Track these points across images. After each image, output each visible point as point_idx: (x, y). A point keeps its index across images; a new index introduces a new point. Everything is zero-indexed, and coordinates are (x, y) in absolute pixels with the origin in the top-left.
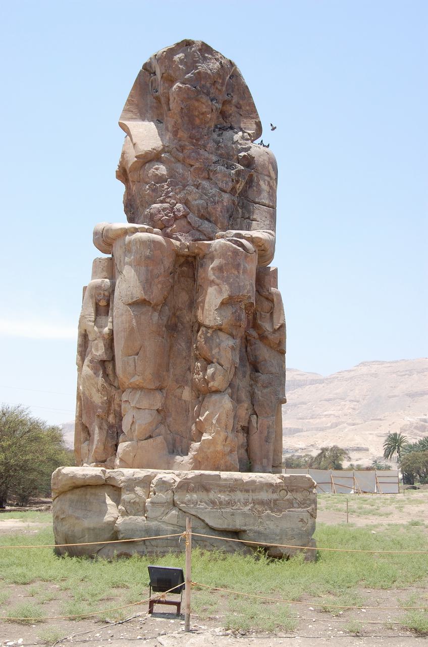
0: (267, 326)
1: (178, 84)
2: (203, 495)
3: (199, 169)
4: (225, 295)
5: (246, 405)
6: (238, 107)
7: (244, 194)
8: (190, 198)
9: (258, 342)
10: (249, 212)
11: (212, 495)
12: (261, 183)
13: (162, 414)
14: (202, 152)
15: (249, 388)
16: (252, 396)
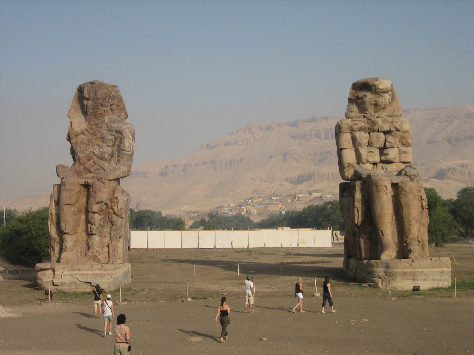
0: (116, 209)
1: (90, 102)
2: (78, 272)
3: (99, 138)
4: (97, 202)
5: (108, 238)
6: (118, 106)
7: (119, 147)
8: (95, 151)
9: (114, 215)
10: (120, 154)
11: (81, 272)
12: (125, 142)
13: (76, 242)
14: (100, 130)
15: (109, 231)
16: (110, 234)
